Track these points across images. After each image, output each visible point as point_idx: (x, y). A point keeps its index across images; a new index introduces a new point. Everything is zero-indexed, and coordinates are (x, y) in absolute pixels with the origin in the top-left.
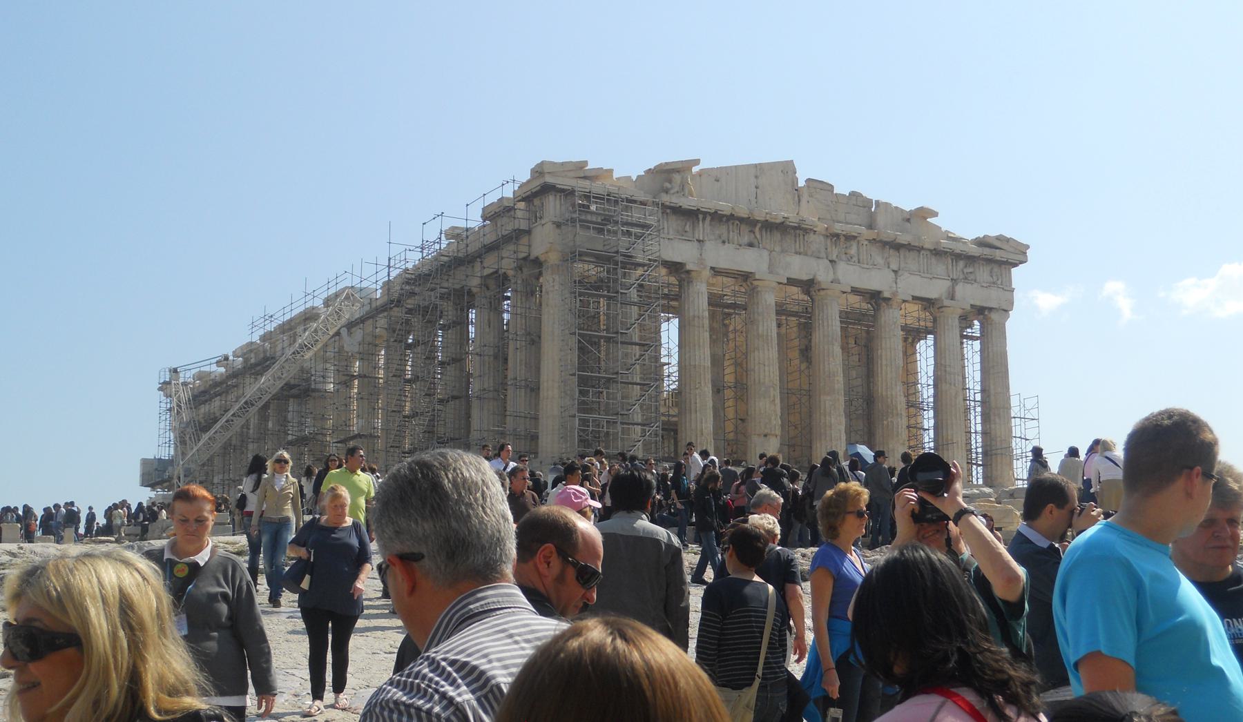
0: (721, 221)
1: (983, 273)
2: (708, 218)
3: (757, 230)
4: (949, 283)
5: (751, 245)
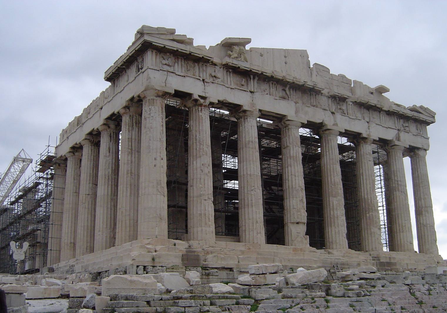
0: (265, 81)
1: (413, 127)
2: (257, 78)
3: (287, 89)
4: (396, 132)
5: (284, 98)
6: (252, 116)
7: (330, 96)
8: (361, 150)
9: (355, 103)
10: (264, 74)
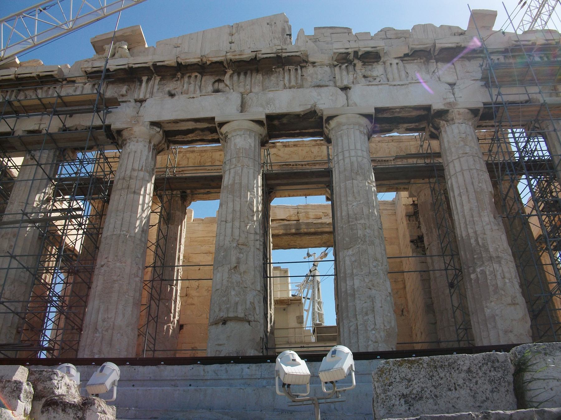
6: (132, 136)
7: (336, 63)
8: (443, 142)
9: (406, 58)
10: (158, 64)
